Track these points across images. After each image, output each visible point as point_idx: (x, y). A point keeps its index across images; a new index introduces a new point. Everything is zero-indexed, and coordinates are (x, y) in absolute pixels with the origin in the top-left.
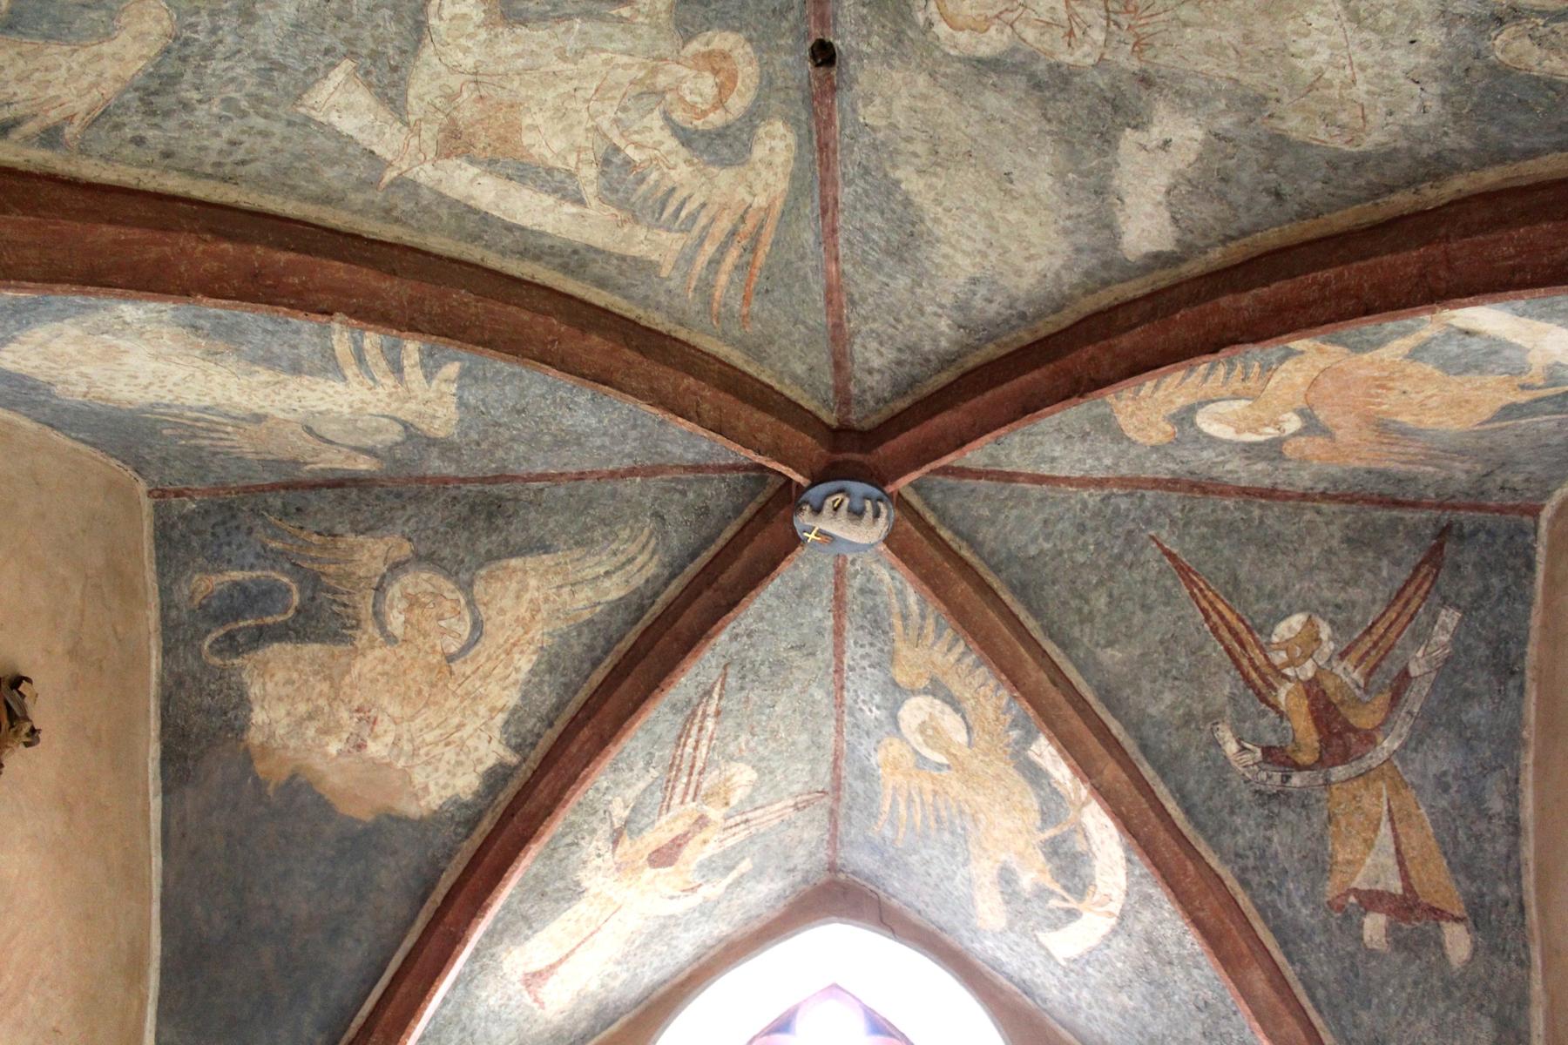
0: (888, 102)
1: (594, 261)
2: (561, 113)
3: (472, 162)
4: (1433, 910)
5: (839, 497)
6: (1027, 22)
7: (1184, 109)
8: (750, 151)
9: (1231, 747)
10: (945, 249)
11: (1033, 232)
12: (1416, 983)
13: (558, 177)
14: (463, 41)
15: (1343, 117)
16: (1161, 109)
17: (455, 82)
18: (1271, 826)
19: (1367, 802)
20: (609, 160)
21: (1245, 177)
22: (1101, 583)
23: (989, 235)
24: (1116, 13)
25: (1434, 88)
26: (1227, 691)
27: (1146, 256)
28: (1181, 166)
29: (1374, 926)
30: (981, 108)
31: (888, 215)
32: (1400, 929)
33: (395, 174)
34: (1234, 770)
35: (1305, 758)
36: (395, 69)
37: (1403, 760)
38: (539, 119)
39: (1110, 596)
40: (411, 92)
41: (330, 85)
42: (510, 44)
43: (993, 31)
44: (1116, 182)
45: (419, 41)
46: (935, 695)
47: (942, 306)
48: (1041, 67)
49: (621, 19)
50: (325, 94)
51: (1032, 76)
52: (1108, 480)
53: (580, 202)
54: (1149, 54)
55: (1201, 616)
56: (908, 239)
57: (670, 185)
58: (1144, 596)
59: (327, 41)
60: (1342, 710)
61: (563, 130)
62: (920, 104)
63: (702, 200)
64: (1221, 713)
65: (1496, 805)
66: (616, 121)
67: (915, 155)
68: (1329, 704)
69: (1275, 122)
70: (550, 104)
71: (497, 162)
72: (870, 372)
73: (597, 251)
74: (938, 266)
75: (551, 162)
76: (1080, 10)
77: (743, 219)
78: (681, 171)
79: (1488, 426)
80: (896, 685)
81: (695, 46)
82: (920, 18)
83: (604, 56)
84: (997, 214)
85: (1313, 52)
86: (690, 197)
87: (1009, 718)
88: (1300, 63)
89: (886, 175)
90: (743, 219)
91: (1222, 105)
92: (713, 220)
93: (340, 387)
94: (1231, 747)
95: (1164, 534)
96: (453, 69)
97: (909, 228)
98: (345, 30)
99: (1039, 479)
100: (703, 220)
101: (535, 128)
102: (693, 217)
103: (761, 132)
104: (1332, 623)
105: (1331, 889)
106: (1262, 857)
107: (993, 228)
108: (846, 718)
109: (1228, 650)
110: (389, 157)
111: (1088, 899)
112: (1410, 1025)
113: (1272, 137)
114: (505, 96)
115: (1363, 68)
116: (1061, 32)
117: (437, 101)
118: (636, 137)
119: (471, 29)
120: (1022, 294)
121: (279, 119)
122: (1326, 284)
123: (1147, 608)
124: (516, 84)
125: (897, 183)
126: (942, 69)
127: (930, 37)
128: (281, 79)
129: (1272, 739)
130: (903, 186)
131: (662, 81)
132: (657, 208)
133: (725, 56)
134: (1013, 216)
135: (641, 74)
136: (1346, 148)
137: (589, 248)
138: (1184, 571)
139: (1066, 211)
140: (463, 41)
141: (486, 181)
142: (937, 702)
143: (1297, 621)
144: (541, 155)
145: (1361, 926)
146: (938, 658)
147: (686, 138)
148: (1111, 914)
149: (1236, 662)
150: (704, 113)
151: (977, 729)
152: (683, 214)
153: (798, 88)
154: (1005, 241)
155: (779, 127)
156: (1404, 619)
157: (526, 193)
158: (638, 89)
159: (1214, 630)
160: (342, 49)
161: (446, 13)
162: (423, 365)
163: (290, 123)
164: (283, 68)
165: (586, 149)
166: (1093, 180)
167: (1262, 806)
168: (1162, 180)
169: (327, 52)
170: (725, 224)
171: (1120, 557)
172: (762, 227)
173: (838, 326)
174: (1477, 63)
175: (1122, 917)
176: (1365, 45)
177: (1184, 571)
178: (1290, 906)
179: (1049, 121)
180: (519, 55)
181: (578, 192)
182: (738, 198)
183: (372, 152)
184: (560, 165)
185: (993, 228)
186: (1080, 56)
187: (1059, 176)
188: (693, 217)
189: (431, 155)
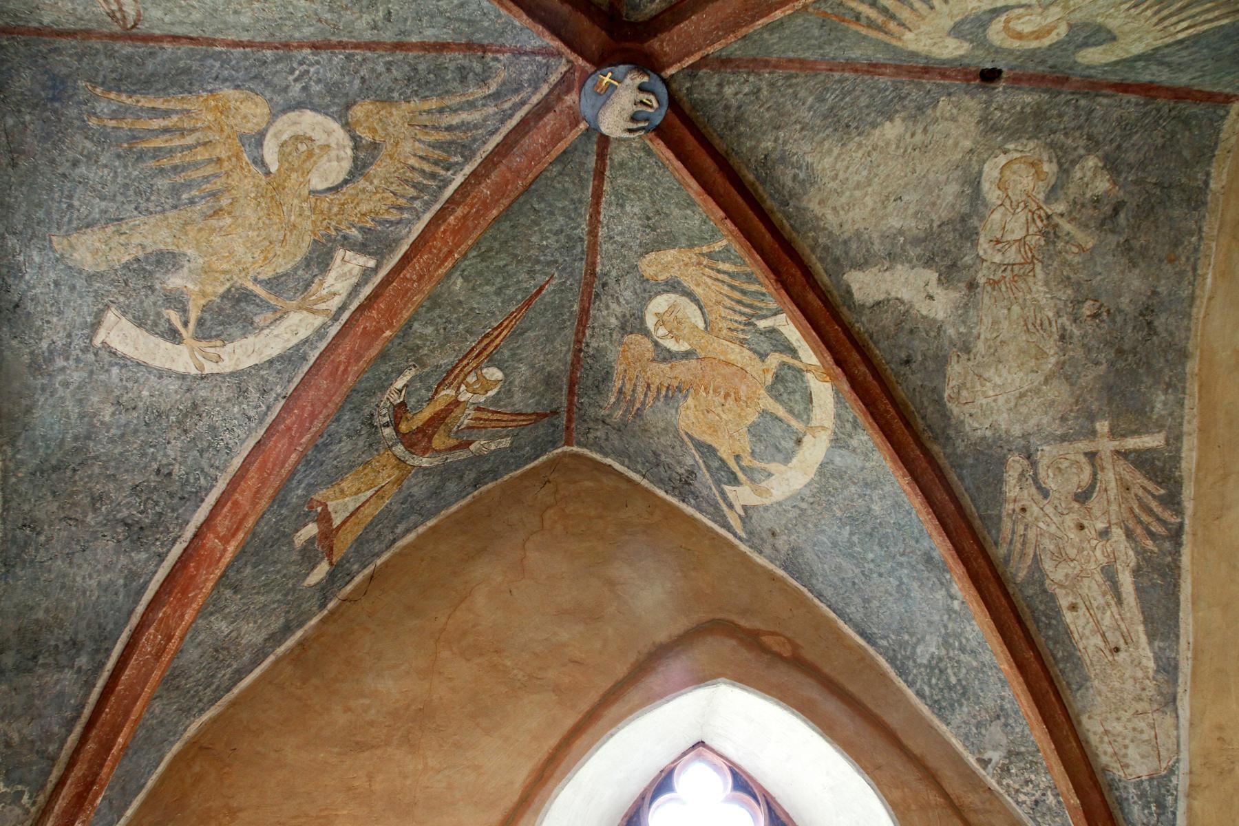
0: (954, 119)
4: (332, 549)
5: (655, 104)
6: (1004, 215)
7: (957, 308)
9: (399, 384)
10: (836, 151)
11: (856, 213)
12: (284, 576)
15: (964, 393)
16: (954, 295)
18: (349, 436)
19: (384, 473)
21: (916, 343)
22: (516, 256)
23: (851, 184)
24: (1012, 270)
25: (989, 433)
26: (441, 362)
27: (848, 286)
28: (917, 306)
29: (312, 529)
30: (947, 182)
31: (866, 111)
32: (313, 543)
34: (383, 395)
35: (404, 427)
37: (416, 473)
39: (505, 266)
43: (1000, 192)
44: (899, 267)
46: (356, 148)
47: (785, 143)
48: (975, 221)
51: (970, 216)
52: (596, 236)
54: (989, 289)
55: (495, 325)
56: (843, 125)
58: (507, 286)
60: (442, 427)
62: (951, 142)
64: (423, 366)
65: (399, 530)
67: (913, 135)
68: (444, 418)
69: (955, 358)
72: (720, 85)
74: (821, 143)
76: (1014, 248)
77: (902, 24)
79: (686, 439)
80: (348, 107)
82: (1011, 146)
84: (870, 190)
85: (1000, 376)
87: (370, 224)
88: (993, 370)
89: (897, 111)
90: (902, 24)
91: (962, 329)
94: (399, 384)
95: (554, 282)
97: (854, 125)
99: (597, 195)
104: (498, 393)
105: (319, 495)
106: (326, 445)
107: (858, 186)
108: (269, 53)
109: (472, 349)
111: (203, 344)
112: (258, 593)
113: (945, 356)
115: (995, 401)
116: (999, 236)
120: (804, 204)
122: (888, 412)
123: (499, 292)
125: (891, 119)
126: (975, 158)
127: (997, 151)
129: (412, 402)
130: (888, 124)
134: (869, 201)
136: (946, 395)
138: (528, 303)
139: (875, 235)
142: (349, 152)
143: (498, 375)
145: (305, 525)
146: (407, 147)
148: (201, 368)
149: (465, 357)
151: (340, 197)
154: (848, 194)
156: (503, 424)
159: (487, 336)
166: (899, 250)
167: (363, 423)
168: (905, 295)
171: (538, 262)
173: (766, 64)
174: (1005, 451)
175: (203, 378)
176: (1007, 401)
177: (528, 303)
178: (299, 482)
179: (940, 226)
185: (858, 186)
186: (984, 245)
187: (901, 232)
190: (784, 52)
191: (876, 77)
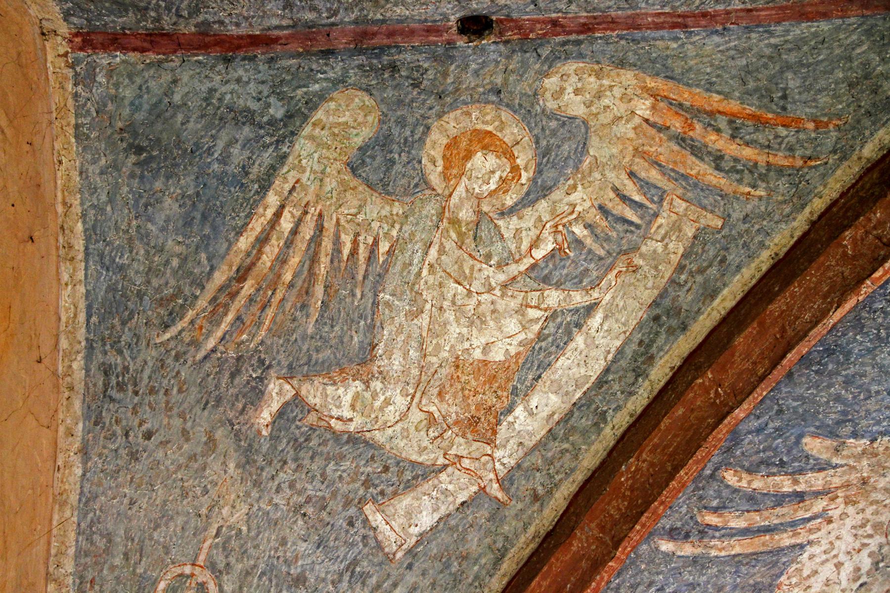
2: (477, 320)
3: (510, 410)
8: (574, 118)
13: (551, 329)
14: (377, 404)
17: (416, 416)
20: (542, 275)
33: (496, 486)
36: (386, 469)
38: (479, 341)
40: (414, 457)
41: (383, 527)
45: (366, 442)
50: (389, 533)
53: (590, 310)
59: (341, 523)
61: (497, 320)
63: (624, 176)
70: (465, 331)
71: (515, 388)
73: (663, 295)
77: (663, 129)
81: (435, 178)
83: (425, 272)
86: (615, 190)
90: (663, 129)
92: (656, 164)
93: (809, 550)
96: (404, 416)
98: (335, 505)
100: (654, 175)
101: (486, 348)
102: (645, 186)
103: (551, 105)
110: (475, 488)
117: (432, 434)
118: (525, 246)
119: (368, 395)
121: (402, 577)
124: (434, 359)
128: (364, 566)
131: (466, 214)
133: (453, 143)
135: (454, 235)
137: (655, 304)
140: (377, 404)
141: (534, 401)
144: (520, 344)
147: (539, 190)
150: (515, 169)
152: (637, 198)
153: (508, 58)
155: (551, 83)
158: (469, 241)
160: (352, 511)
161: (347, 414)
162: (801, 471)
163: (410, 567)
164: (355, 562)
169: (351, 524)
170: (666, 150)
172: (681, 105)
180: (406, 355)
181: (577, 310)
182: (631, 134)
183: (463, 504)
184: (536, 328)
188: (645, 186)
190: (838, 29)
191: (667, 10)
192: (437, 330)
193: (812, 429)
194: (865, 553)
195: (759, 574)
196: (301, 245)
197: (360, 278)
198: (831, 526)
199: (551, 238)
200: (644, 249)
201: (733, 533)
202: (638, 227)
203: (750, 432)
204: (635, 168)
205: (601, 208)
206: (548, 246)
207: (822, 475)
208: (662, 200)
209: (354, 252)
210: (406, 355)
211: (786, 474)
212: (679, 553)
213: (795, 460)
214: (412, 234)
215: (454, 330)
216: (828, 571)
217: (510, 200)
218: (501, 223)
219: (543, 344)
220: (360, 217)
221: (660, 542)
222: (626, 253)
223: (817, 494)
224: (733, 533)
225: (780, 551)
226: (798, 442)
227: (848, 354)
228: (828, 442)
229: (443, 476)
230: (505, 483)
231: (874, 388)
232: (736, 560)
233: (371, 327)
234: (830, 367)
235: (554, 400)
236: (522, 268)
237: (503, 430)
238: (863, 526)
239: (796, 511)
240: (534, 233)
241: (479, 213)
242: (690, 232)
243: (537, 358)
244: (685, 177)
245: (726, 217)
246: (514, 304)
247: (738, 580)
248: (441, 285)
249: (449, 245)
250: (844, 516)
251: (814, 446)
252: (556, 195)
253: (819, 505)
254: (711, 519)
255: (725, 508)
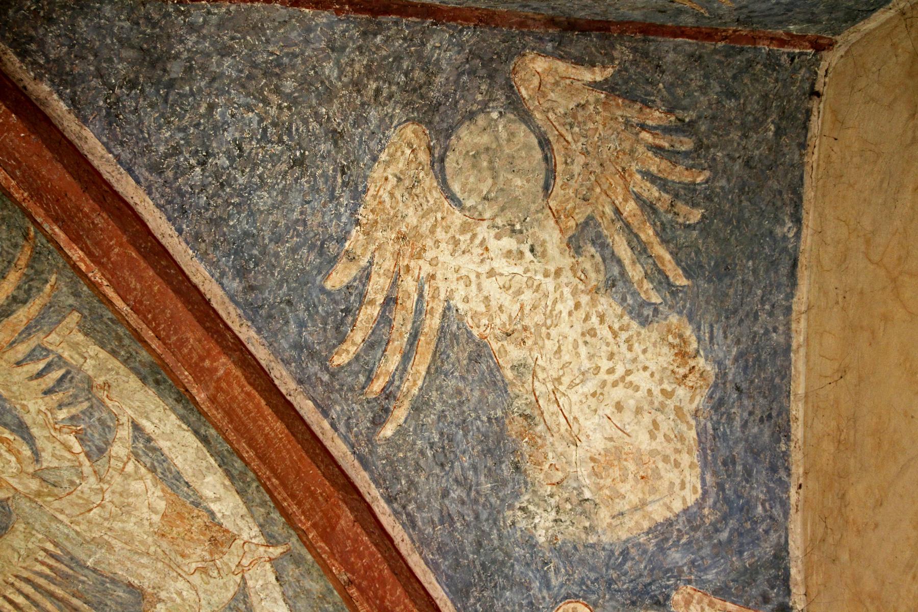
1: (143, 364)
2: (126, 509)
3: (212, 514)
14: (178, 600)
17: (196, 579)
33: (271, 549)
38: (145, 513)
40: (230, 595)
42: (146, 577)
49: (56, 545)
53: (136, 427)
57: (47, 399)
61: (129, 495)
63: (19, 370)
66: (82, 477)
70: (133, 519)
71: (192, 503)
75: (150, 476)
78: (34, 408)
83: (77, 528)
86: (31, 378)
92: (11, 345)
93: (457, 302)
96: (194, 587)
100: (22, 349)
102: (31, 357)
110: (268, 566)
114: (164, 544)
117: (215, 574)
118: (68, 455)
119: (169, 605)
131: (34, 485)
132: (66, 382)
135: (49, 499)
137: (143, 380)
141: (208, 493)
144: (155, 486)
152: (41, 365)
157: (179, 462)
158: (56, 491)
162: (362, 295)
165: (115, 469)
180: (144, 566)
181: (135, 439)
183: (277, 579)
184: (143, 470)
188: (31, 357)
189: (239, 542)
192: (128, 538)
193: (319, 278)
194: (493, 244)
195: (459, 354)
196: (38, 597)
197: (71, 572)
198: (439, 276)
199: (65, 436)
200: (90, 373)
201: (403, 369)
202: (68, 372)
203: (300, 334)
204: (13, 360)
205: (48, 392)
206: (72, 440)
207: (374, 277)
208: (46, 349)
209: (50, 567)
210: (144, 566)
211: (359, 309)
212: (401, 421)
213: (346, 299)
214: (43, 525)
215: (130, 526)
216: (491, 286)
217: (26, 452)
218: (45, 465)
219: (159, 470)
220: (22, 552)
221: (381, 435)
222: (91, 387)
223: (394, 284)
224: (403, 369)
225: (442, 331)
226: (329, 293)
227: (246, 234)
228: (339, 266)
229: (250, 583)
230: (271, 541)
231: (296, 215)
232: (435, 371)
233: (113, 581)
234: (255, 252)
235: (209, 479)
236: (87, 463)
237: (227, 524)
238: (456, 243)
239: (404, 308)
240: (57, 444)
241: (34, 475)
242: (80, 337)
243: (170, 478)
244: (28, 328)
245: (73, 308)
246: (118, 479)
247: (456, 374)
248: (90, 522)
249: (56, 504)
250: (433, 262)
251: (339, 278)
252: (28, 419)
253: (409, 284)
254: (377, 386)
255: (371, 371)
